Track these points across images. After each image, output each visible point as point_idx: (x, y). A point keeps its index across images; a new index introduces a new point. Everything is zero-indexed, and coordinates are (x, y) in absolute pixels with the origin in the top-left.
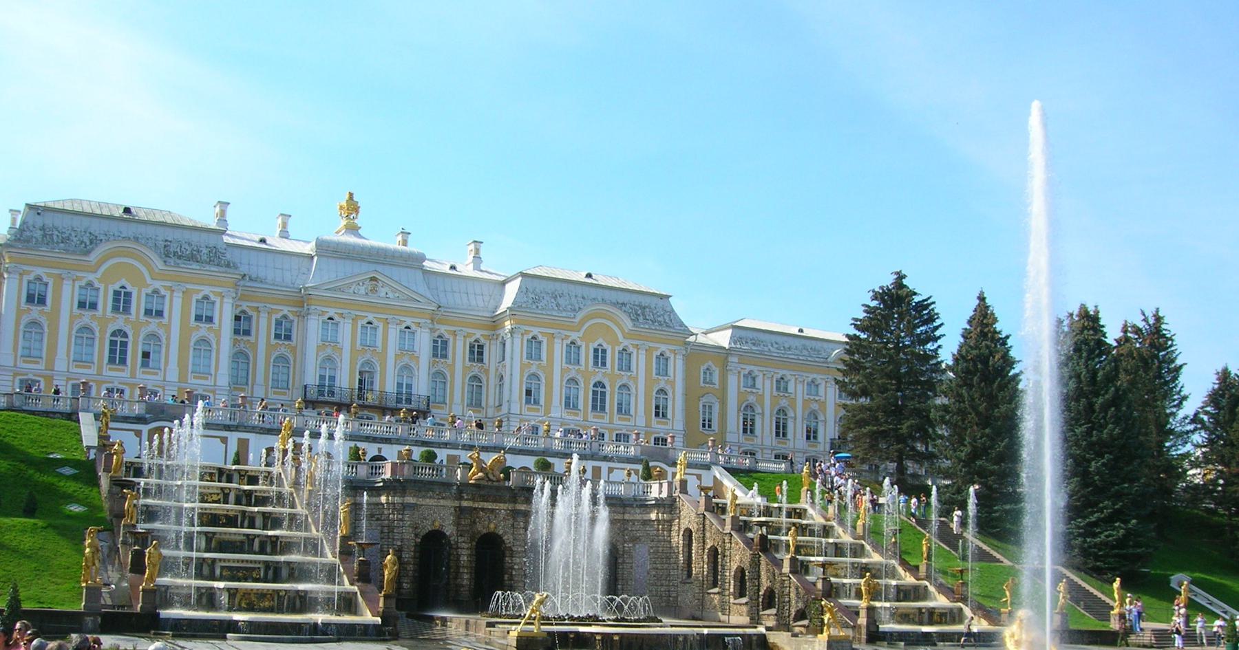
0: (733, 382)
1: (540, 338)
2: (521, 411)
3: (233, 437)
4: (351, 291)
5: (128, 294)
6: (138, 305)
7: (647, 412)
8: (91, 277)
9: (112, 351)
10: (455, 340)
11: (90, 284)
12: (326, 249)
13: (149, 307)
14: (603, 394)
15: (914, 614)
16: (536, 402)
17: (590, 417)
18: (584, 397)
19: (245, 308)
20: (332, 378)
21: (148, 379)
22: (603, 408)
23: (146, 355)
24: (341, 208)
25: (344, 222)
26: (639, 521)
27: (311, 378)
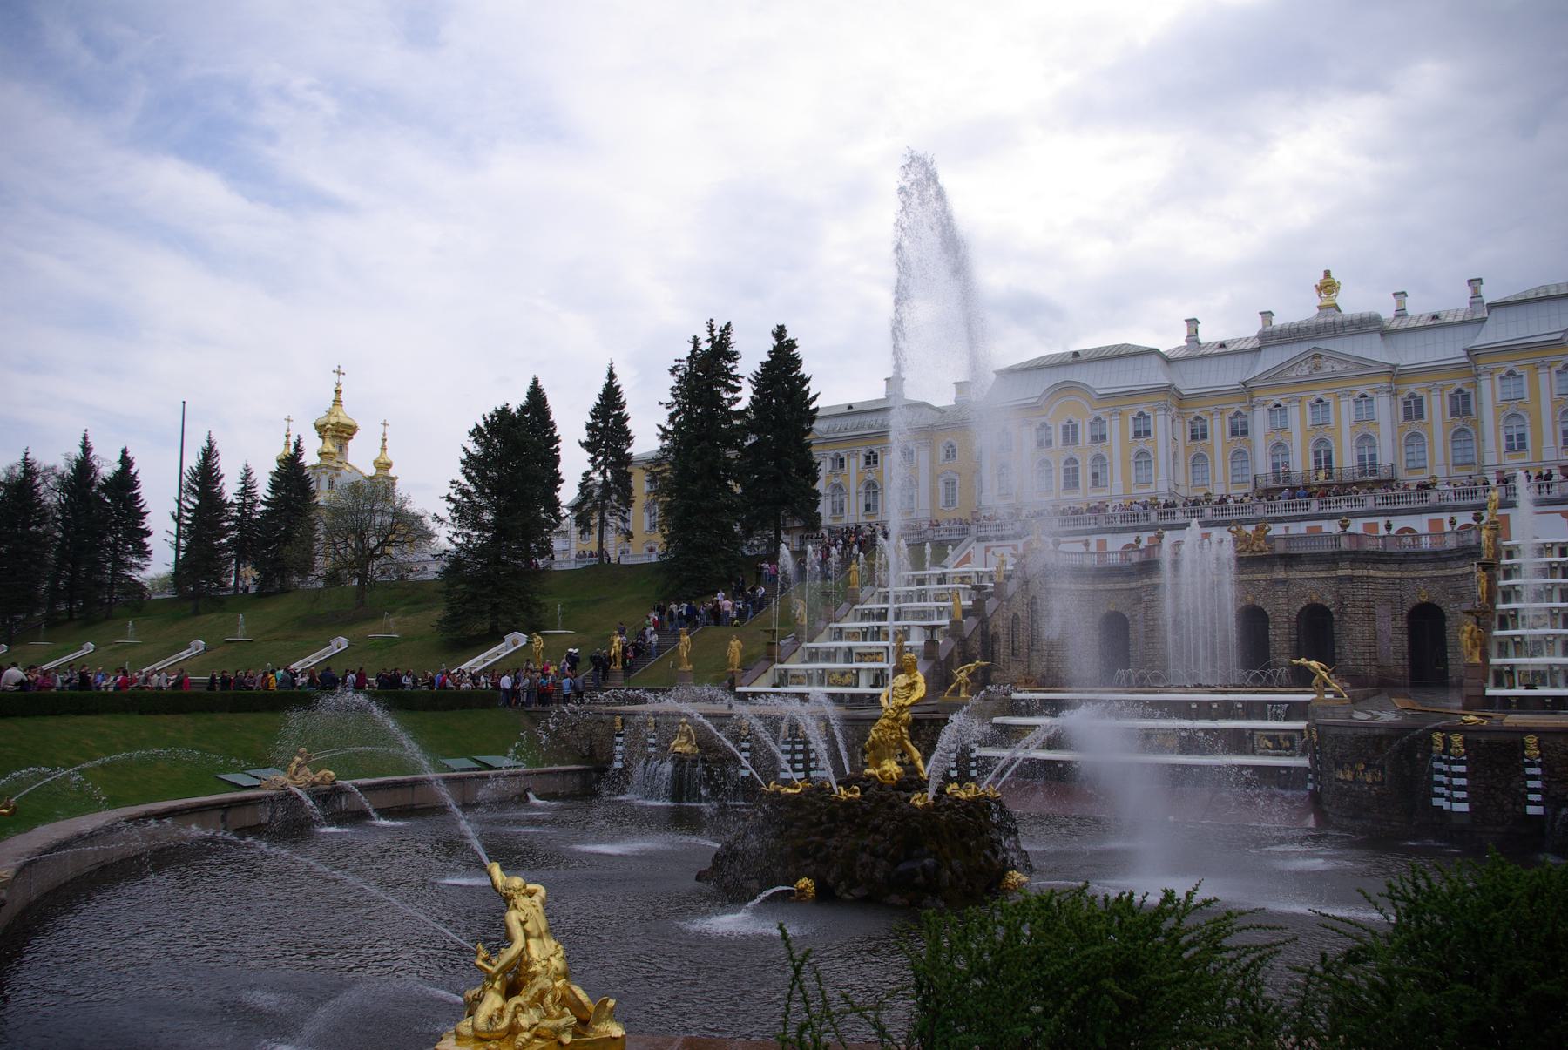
2: (1499, 459)
3: (1093, 539)
4: (1294, 374)
5: (1075, 427)
6: (1084, 434)
9: (1066, 478)
12: (1272, 338)
16: (1522, 446)
19: (1197, 414)
20: (1286, 464)
21: (1096, 497)
23: (1095, 476)
24: (1318, 289)
25: (1318, 302)
26: (1461, 575)
27: (1262, 465)
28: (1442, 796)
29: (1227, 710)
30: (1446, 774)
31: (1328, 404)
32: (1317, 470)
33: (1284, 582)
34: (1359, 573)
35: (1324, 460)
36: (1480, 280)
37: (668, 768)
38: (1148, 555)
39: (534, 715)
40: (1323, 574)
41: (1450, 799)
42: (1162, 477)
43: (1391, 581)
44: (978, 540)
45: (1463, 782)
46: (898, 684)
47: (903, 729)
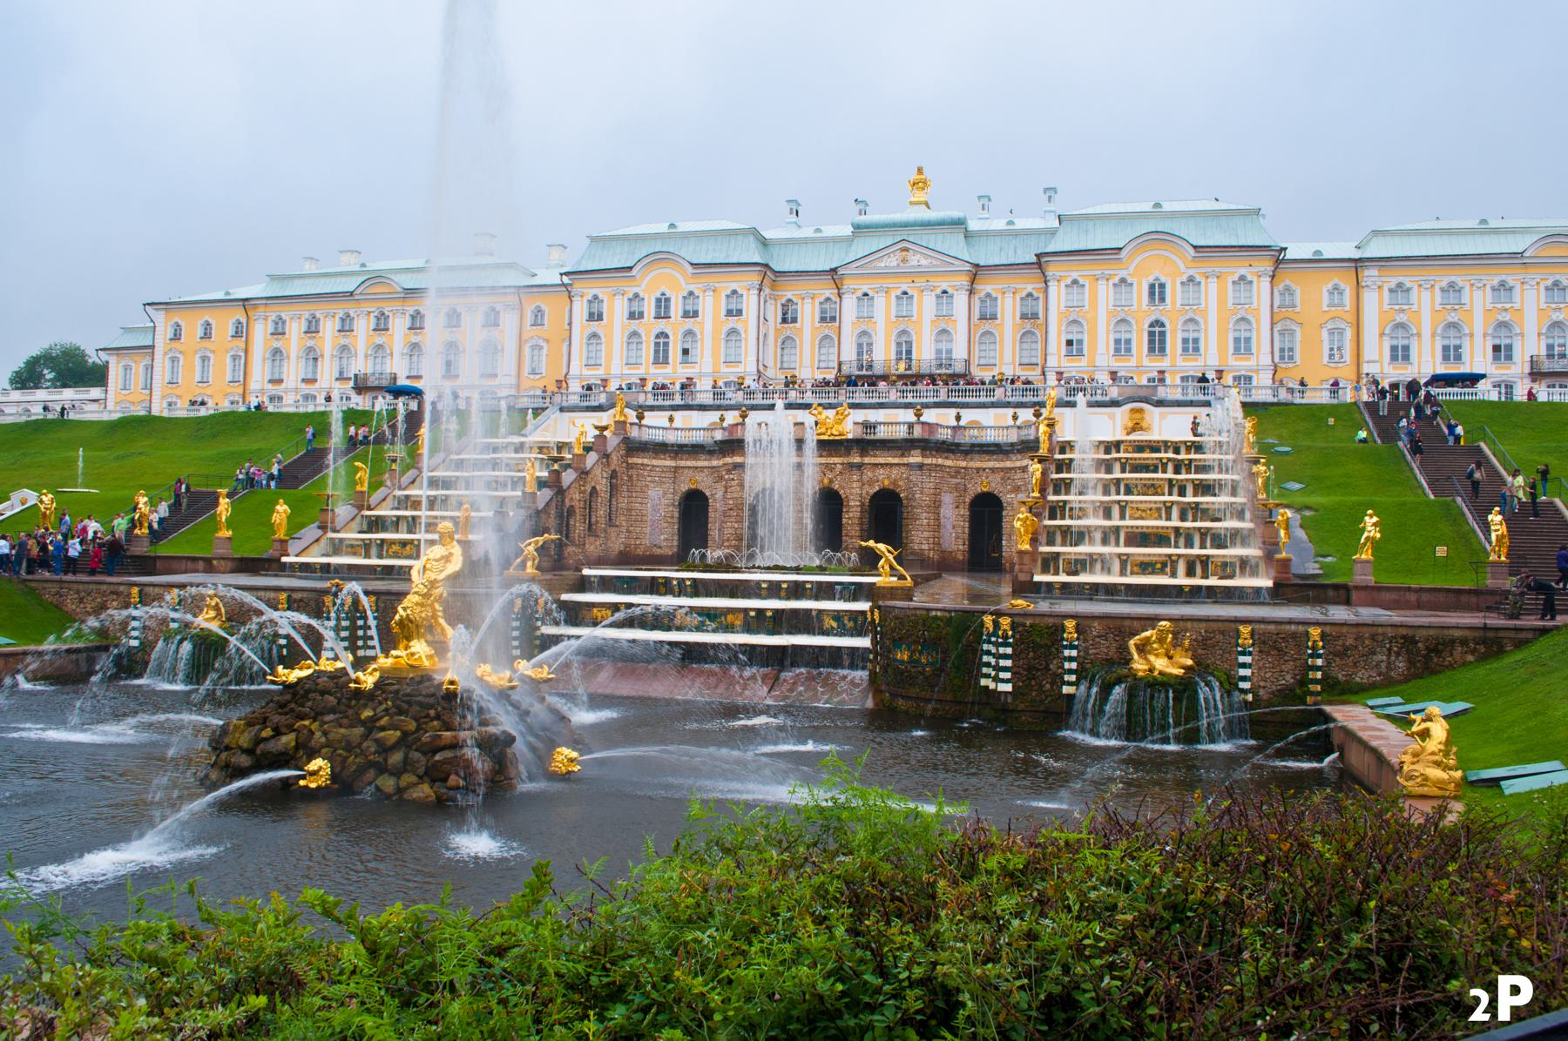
0: (1371, 300)
1: (1081, 281)
5: (668, 300)
6: (676, 309)
7: (1222, 349)
8: (636, 290)
9: (657, 352)
10: (1003, 298)
11: (636, 296)
13: (688, 308)
14: (1162, 334)
15: (1164, 565)
16: (1080, 353)
17: (1146, 362)
18: (1140, 341)
22: (1162, 350)
23: (686, 352)
27: (849, 354)
28: (987, 676)
29: (797, 591)
30: (994, 655)
31: (912, 297)
32: (899, 359)
33: (860, 466)
34: (928, 461)
35: (905, 352)
36: (1054, 190)
37: (187, 647)
38: (731, 433)
39: (34, 585)
40: (896, 461)
41: (996, 679)
42: (752, 358)
43: (958, 471)
44: (562, 410)
45: (1008, 663)
46: (431, 557)
47: (437, 606)
